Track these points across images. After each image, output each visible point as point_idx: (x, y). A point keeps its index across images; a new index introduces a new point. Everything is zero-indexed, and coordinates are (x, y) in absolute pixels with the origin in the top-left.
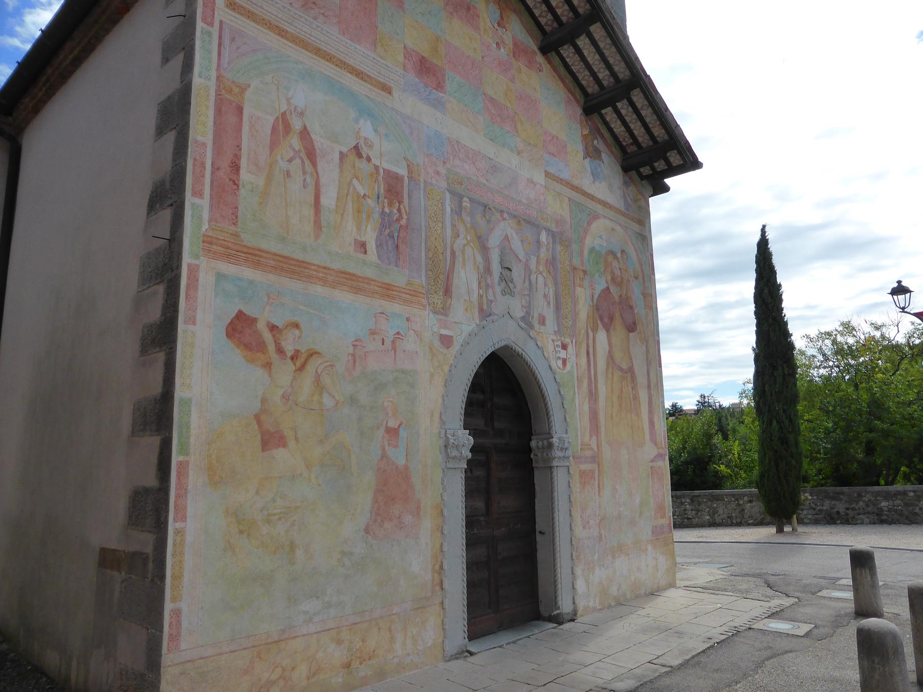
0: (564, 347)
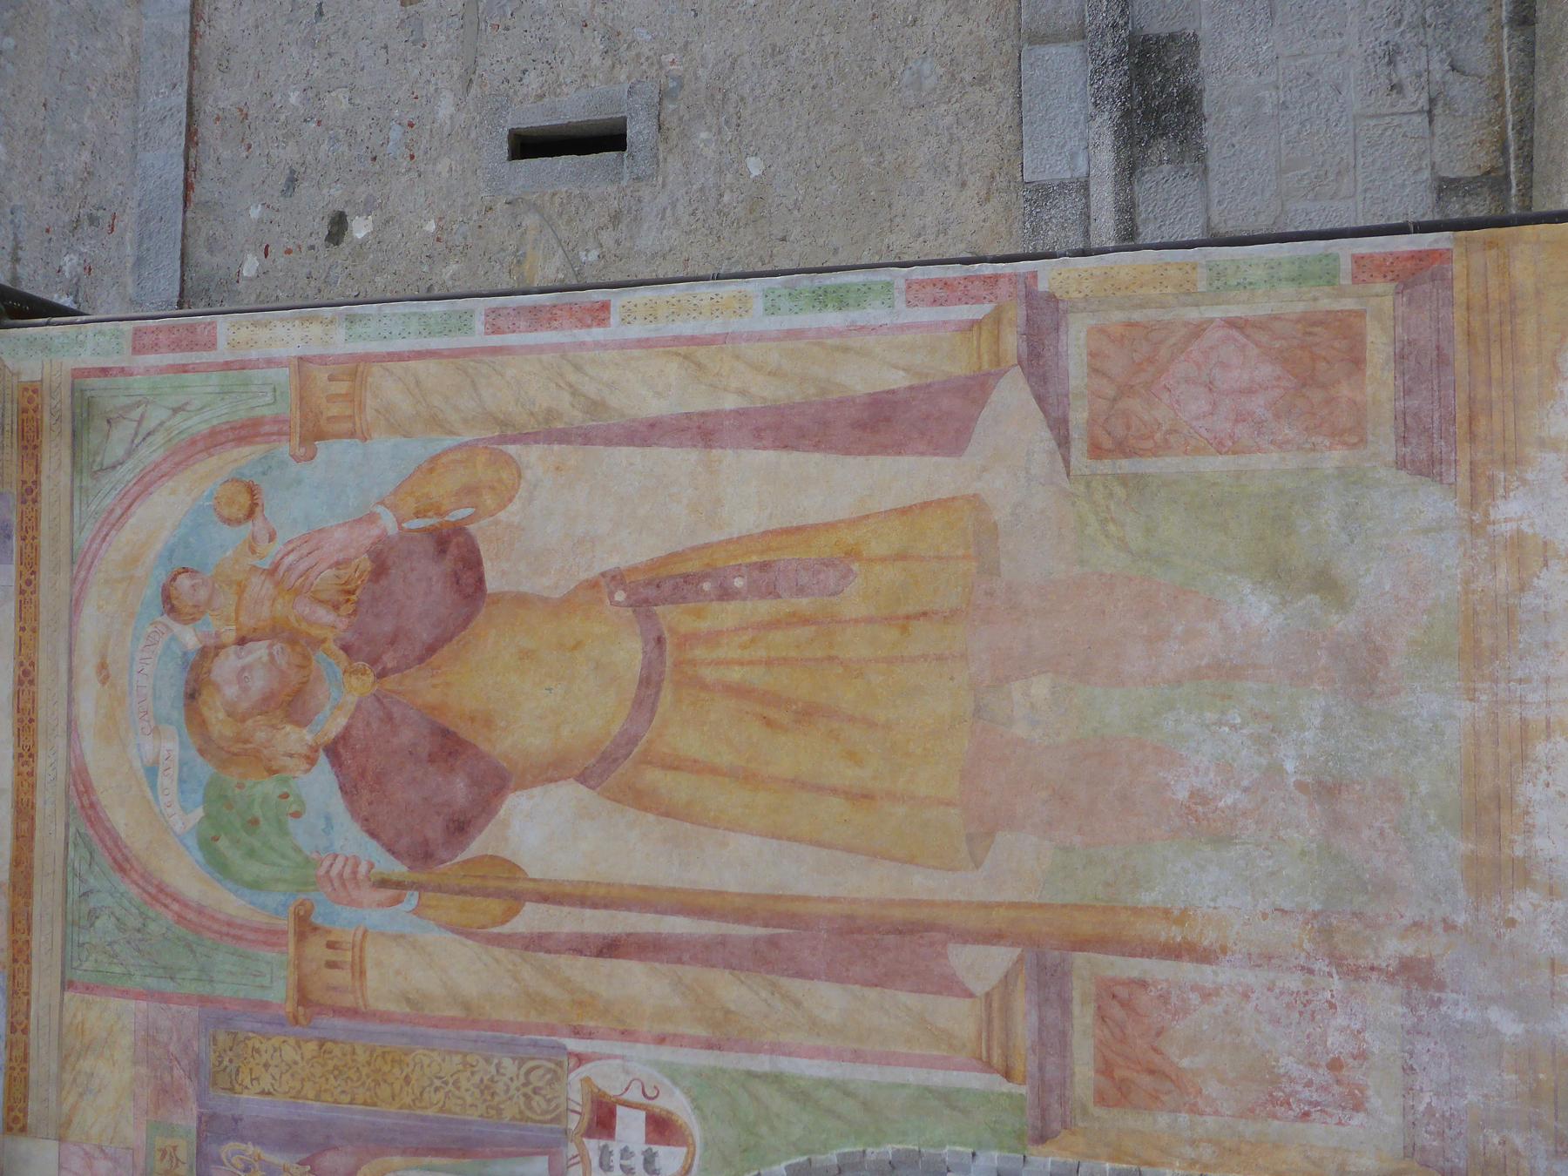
0: (603, 1119)
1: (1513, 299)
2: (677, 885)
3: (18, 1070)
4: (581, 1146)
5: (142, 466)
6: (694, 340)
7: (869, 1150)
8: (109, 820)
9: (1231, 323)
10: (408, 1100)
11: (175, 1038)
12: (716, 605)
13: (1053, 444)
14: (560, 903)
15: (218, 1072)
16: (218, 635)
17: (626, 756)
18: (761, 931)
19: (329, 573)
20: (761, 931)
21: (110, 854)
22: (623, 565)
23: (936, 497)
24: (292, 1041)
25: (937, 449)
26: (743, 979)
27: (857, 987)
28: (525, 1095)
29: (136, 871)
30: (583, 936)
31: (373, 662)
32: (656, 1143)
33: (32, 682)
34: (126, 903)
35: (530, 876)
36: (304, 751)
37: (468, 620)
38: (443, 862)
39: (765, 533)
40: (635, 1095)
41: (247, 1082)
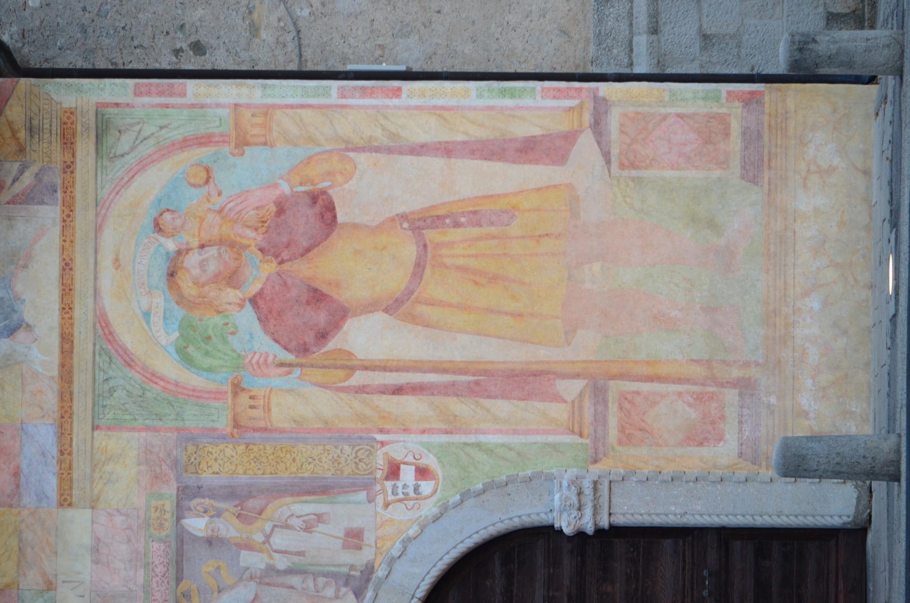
0: (394, 471)
1: (786, 113)
2: (431, 359)
3: (66, 474)
4: (383, 485)
5: (140, 156)
6: (442, 108)
7: (520, 474)
8: (121, 340)
9: (679, 115)
10: (294, 470)
11: (163, 450)
12: (452, 230)
13: (604, 163)
14: (374, 370)
15: (188, 465)
16: (188, 243)
17: (408, 300)
18: (471, 378)
19: (252, 212)
20: (471, 378)
21: (122, 358)
22: (407, 211)
23: (553, 184)
24: (231, 446)
25: (554, 163)
26: (463, 400)
27: (515, 401)
28: (355, 463)
29: (138, 366)
30: (385, 385)
31: (276, 257)
32: (421, 480)
33: (71, 269)
36: (238, 301)
37: (328, 235)
38: (314, 353)
39: (476, 197)
40: (410, 459)
41: (205, 468)
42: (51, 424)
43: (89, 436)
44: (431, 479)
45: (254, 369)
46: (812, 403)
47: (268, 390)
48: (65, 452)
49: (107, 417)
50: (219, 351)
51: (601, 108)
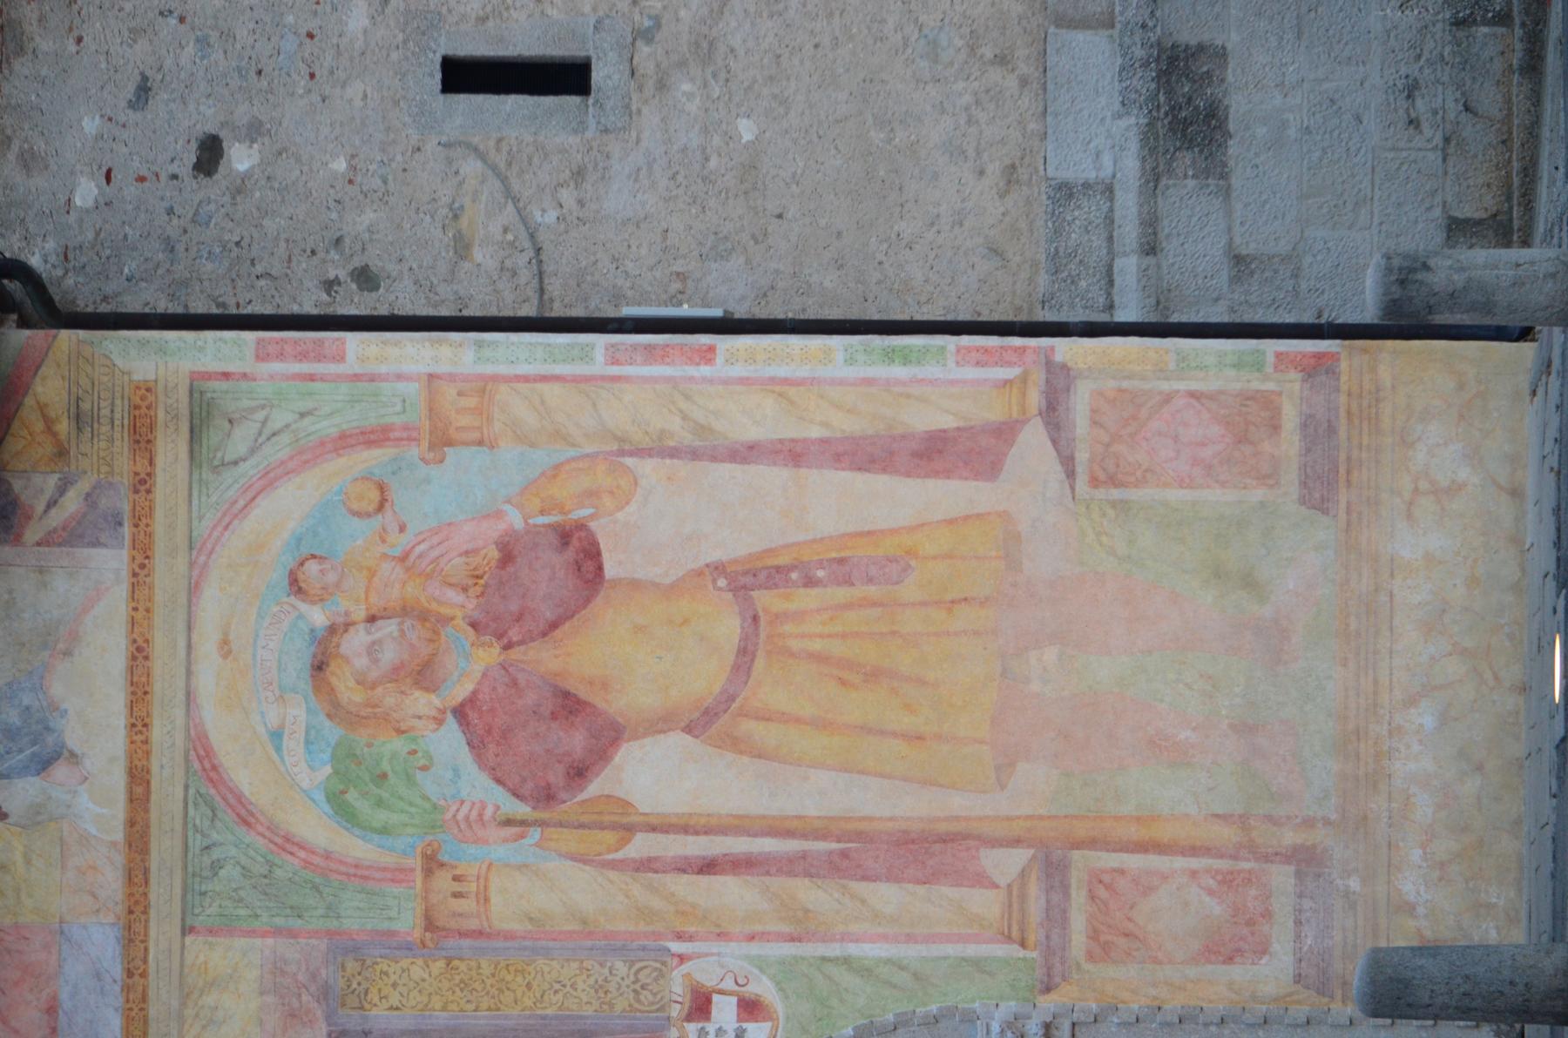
0: (701, 1006)
1: (1378, 390)
3: (136, 1010)
6: (786, 381)
7: (918, 1010)
8: (232, 780)
9: (1192, 395)
10: (529, 1003)
11: (304, 968)
12: (802, 591)
13: (1063, 476)
14: (667, 832)
16: (347, 614)
18: (834, 846)
20: (834, 846)
21: (234, 810)
22: (724, 558)
23: (976, 511)
24: (420, 962)
25: (977, 475)
26: (819, 884)
27: (910, 886)
28: (635, 991)
29: (262, 824)
30: (686, 858)
31: (500, 637)
32: (747, 1021)
33: (146, 658)
34: (252, 853)
35: (641, 811)
36: (434, 713)
37: (587, 601)
38: (564, 802)
39: (844, 535)
40: (729, 984)
41: (376, 1000)
42: (113, 924)
43: (176, 946)
44: (764, 1020)
45: (461, 831)
46: (1422, 889)
47: (484, 867)
48: (135, 972)
49: (208, 912)
50: (401, 798)
51: (1058, 384)
